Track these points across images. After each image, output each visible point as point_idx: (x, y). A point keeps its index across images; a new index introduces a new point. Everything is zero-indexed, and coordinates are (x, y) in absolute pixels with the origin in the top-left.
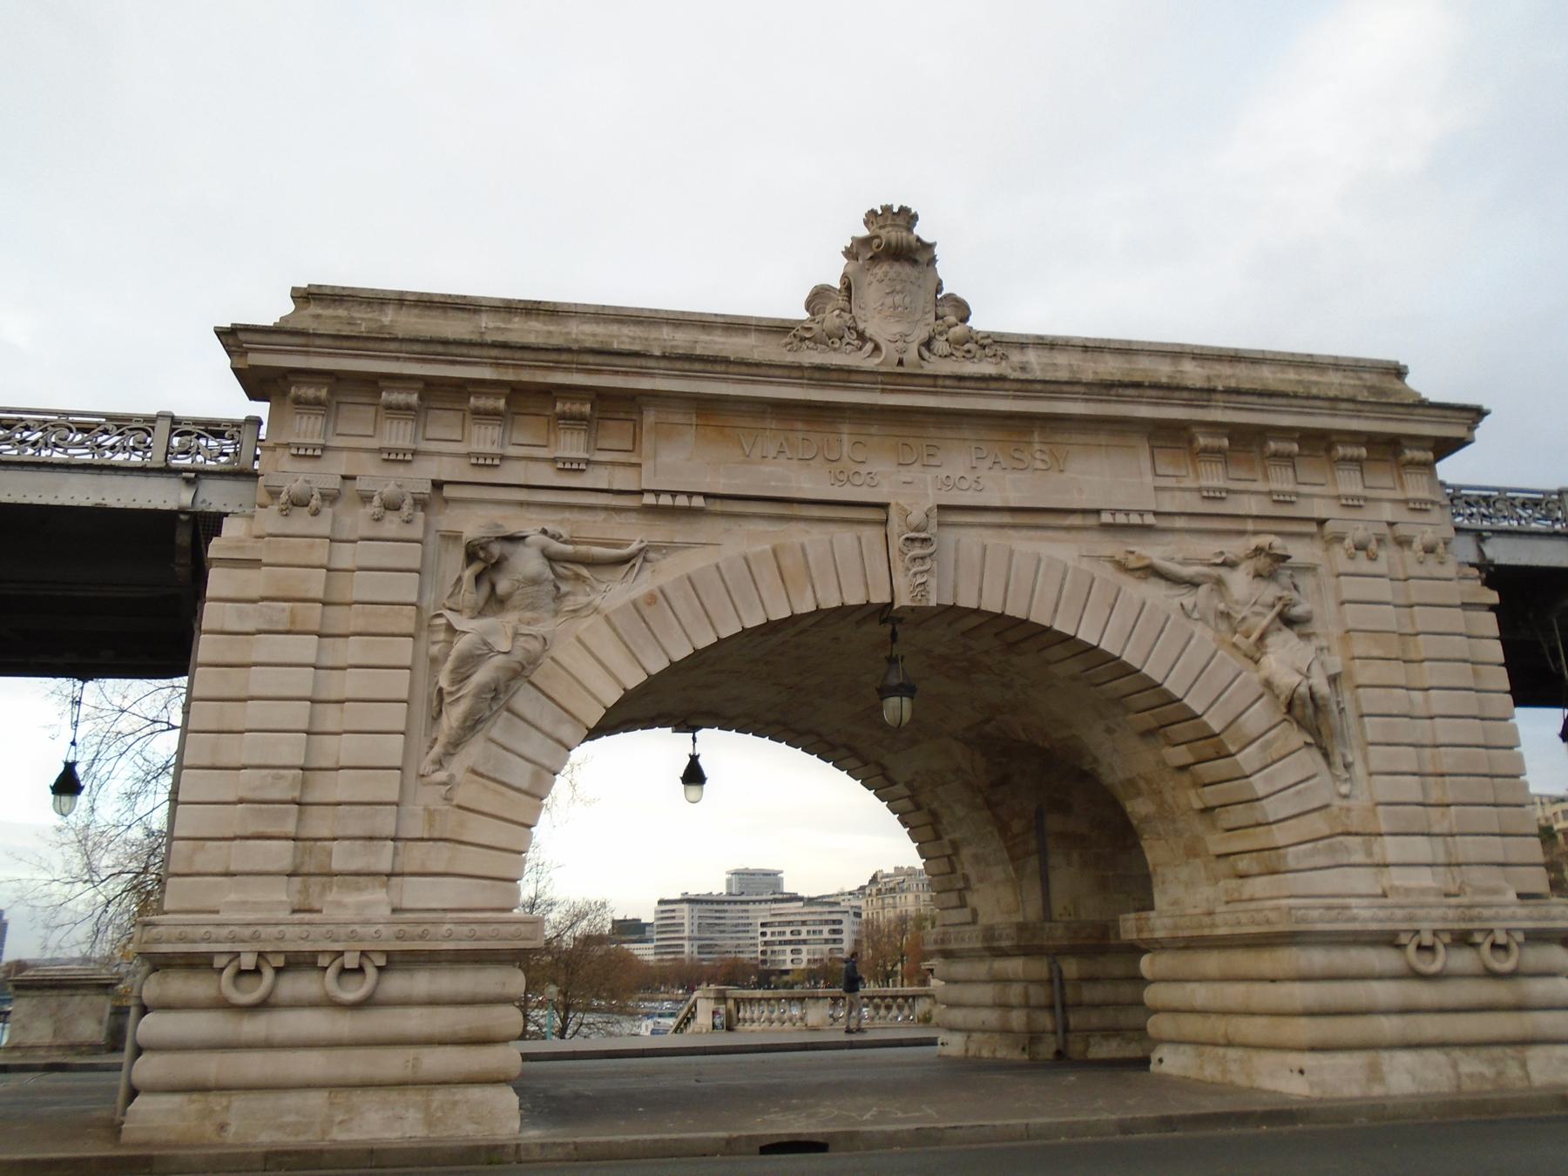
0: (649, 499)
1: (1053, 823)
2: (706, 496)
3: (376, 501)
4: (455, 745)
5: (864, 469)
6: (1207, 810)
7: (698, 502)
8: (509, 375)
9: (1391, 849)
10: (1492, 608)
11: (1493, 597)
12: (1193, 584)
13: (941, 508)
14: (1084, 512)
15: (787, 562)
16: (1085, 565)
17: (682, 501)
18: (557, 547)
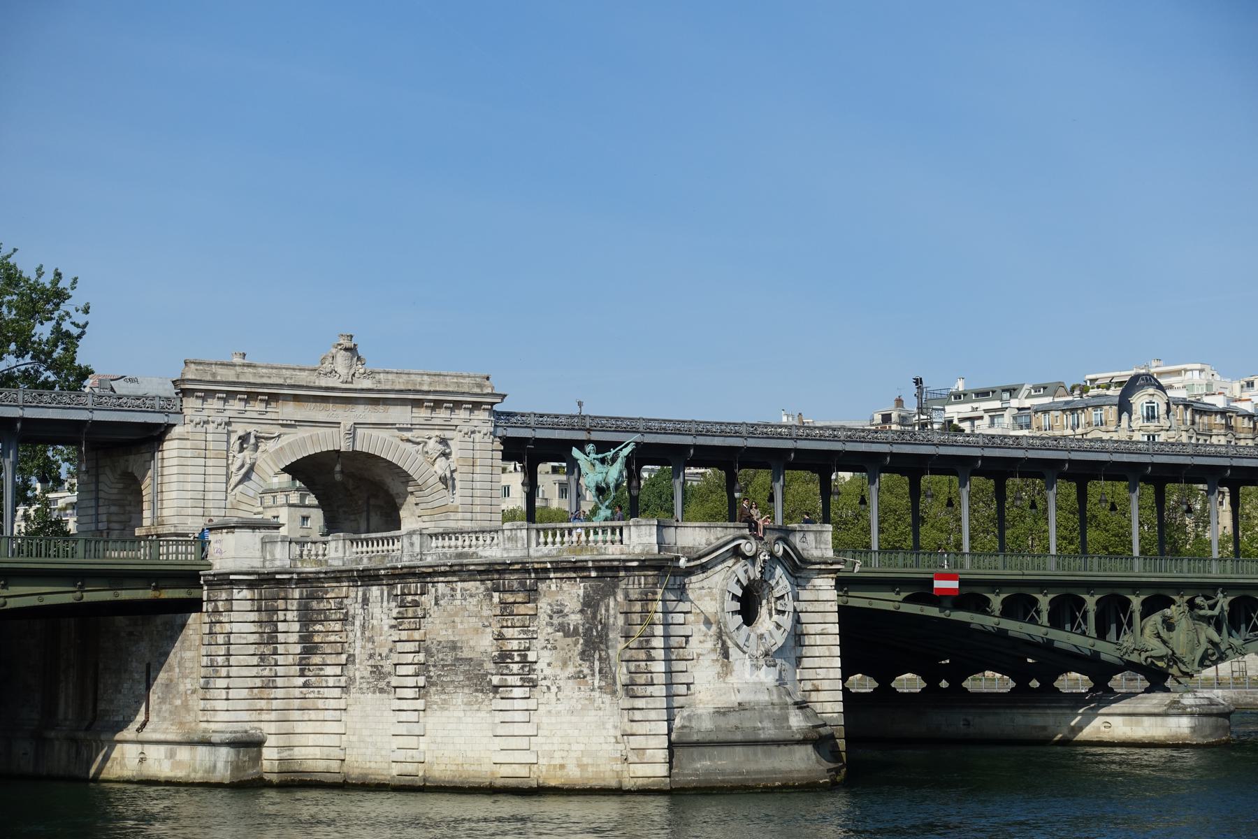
0: (281, 422)
1: (372, 501)
2: (295, 421)
3: (216, 423)
4: (236, 486)
5: (335, 413)
6: (417, 504)
7: (293, 422)
8: (249, 390)
9: (460, 516)
10: (501, 450)
11: (502, 448)
12: (418, 443)
13: (355, 424)
14: (392, 424)
15: (314, 438)
16: (391, 439)
17: (289, 422)
18: (258, 434)
